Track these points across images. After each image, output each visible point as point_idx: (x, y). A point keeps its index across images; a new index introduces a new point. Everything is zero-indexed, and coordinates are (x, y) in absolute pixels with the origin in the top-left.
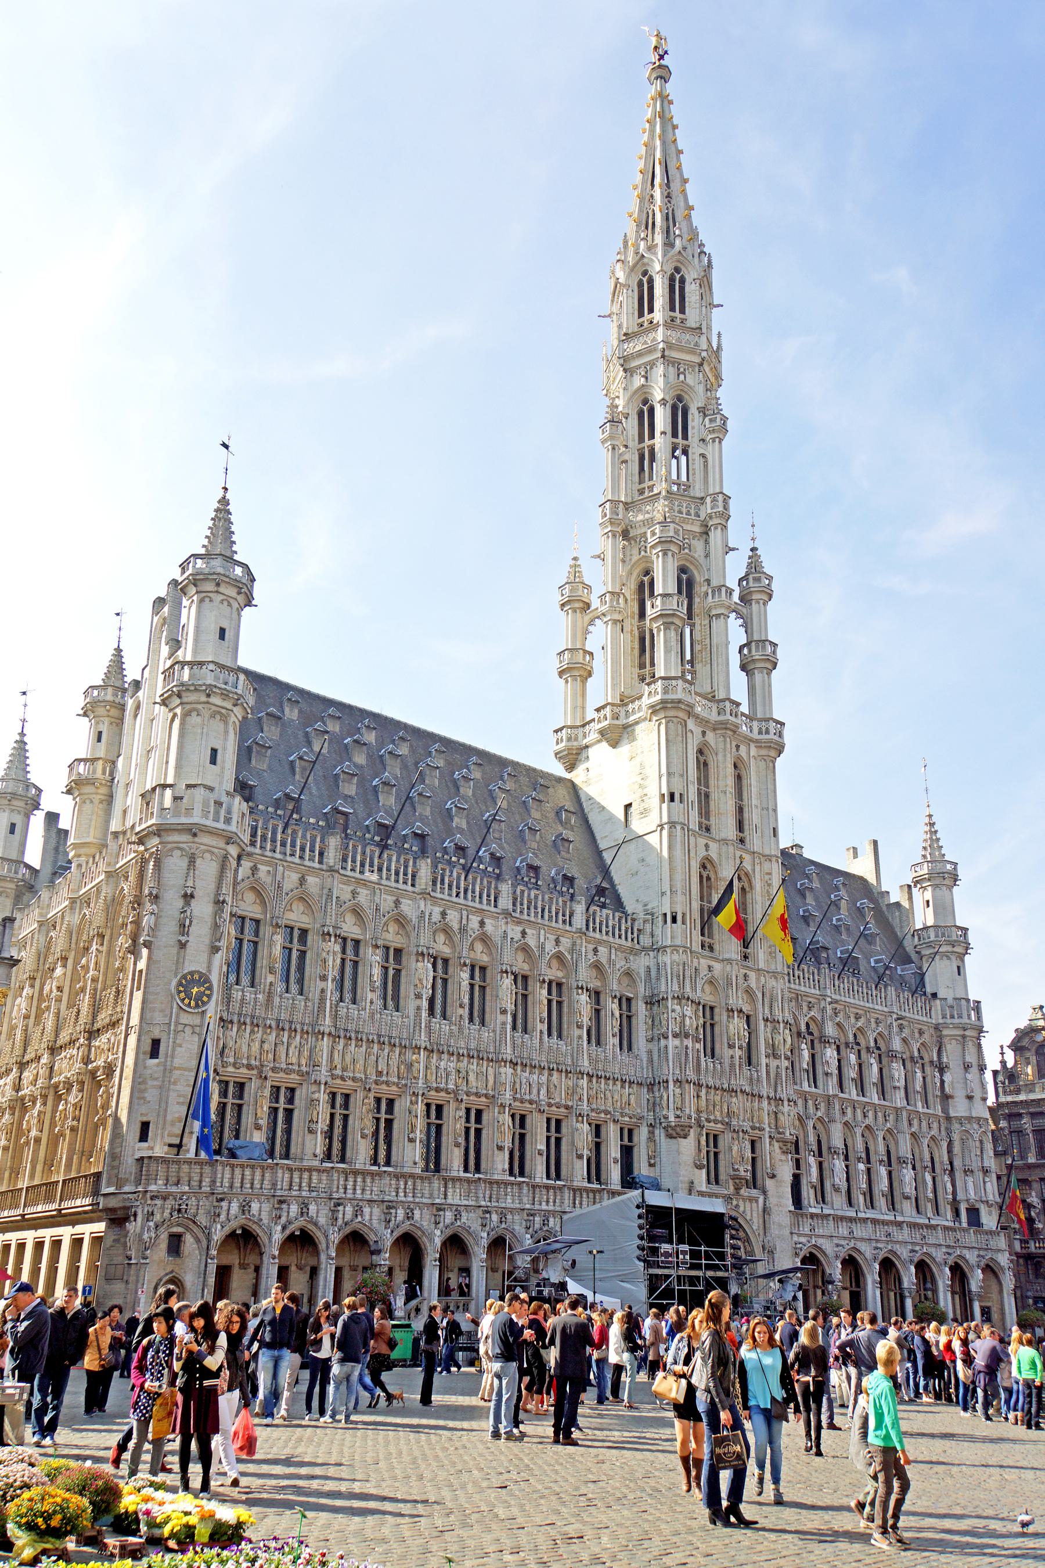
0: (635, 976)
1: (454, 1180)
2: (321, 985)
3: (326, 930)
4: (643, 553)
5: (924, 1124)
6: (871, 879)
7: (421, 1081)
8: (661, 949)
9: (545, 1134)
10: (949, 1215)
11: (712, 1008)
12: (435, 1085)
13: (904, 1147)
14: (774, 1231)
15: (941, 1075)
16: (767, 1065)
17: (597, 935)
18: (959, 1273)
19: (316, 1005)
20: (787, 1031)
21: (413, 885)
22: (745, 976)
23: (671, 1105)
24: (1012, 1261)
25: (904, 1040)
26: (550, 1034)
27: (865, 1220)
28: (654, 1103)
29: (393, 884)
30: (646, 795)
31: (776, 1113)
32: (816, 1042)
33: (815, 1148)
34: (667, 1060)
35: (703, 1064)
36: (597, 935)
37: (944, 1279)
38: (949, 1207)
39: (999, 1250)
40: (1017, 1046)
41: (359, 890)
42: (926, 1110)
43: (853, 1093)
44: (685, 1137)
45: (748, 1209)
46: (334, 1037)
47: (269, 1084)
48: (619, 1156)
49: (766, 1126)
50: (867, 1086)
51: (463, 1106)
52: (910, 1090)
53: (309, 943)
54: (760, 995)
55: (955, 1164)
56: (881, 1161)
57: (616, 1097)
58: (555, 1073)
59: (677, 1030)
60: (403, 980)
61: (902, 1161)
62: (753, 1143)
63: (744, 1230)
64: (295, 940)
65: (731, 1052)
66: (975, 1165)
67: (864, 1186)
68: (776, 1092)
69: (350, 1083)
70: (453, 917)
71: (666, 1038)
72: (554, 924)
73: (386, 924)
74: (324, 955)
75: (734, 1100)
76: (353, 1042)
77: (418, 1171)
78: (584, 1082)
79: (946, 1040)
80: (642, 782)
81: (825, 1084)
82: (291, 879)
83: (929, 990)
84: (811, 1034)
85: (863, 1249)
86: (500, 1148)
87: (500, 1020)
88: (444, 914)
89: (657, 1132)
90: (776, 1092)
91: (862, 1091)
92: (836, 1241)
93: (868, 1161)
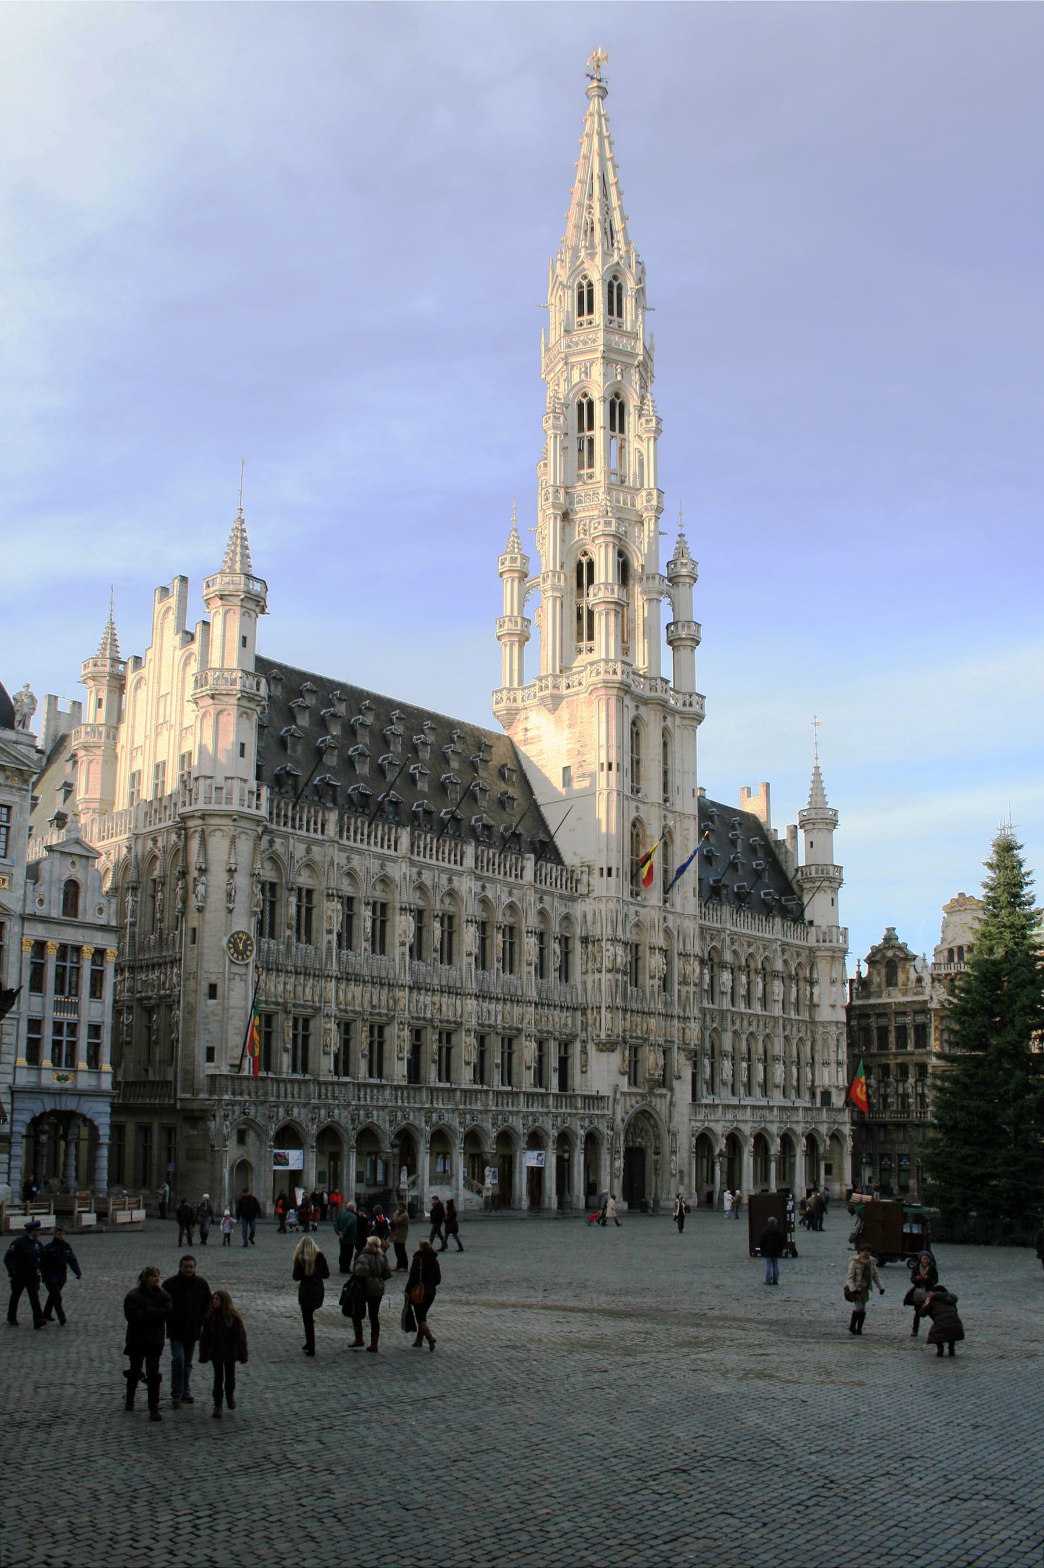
0: (573, 919)
1: (432, 1090)
2: (326, 937)
3: (330, 892)
5: (794, 1029)
6: (762, 819)
9: (500, 1050)
10: (807, 1097)
12: (416, 1015)
13: (778, 1047)
14: (676, 1118)
15: (811, 988)
16: (679, 991)
18: (812, 1140)
20: (697, 963)
21: (396, 850)
22: (665, 918)
24: (852, 1130)
25: (785, 962)
27: (745, 1107)
29: (379, 850)
32: (715, 967)
33: (709, 1052)
34: (600, 991)
36: (543, 887)
37: (801, 1147)
38: (808, 1092)
39: (844, 1123)
40: (871, 961)
41: (352, 856)
42: (797, 1017)
43: (742, 1007)
44: (613, 1051)
46: (338, 979)
47: (291, 1016)
48: (557, 1065)
49: (676, 1040)
51: (437, 1031)
52: (786, 1002)
54: (676, 933)
55: (816, 1058)
56: (759, 1060)
57: (557, 1019)
60: (388, 929)
61: (776, 1059)
62: (664, 1052)
63: (655, 1120)
64: (304, 900)
65: (652, 982)
66: (833, 1057)
67: (745, 1079)
68: (684, 1011)
70: (427, 877)
71: (600, 972)
72: (509, 879)
75: (653, 1020)
76: (353, 983)
77: (405, 1083)
78: (532, 1009)
79: (818, 960)
80: (581, 749)
81: (721, 1001)
82: (300, 850)
83: (808, 916)
84: (711, 960)
86: (468, 1063)
87: (465, 962)
88: (419, 874)
89: (589, 1046)
90: (684, 1011)
91: (749, 1004)
92: (723, 1123)
93: (749, 1059)
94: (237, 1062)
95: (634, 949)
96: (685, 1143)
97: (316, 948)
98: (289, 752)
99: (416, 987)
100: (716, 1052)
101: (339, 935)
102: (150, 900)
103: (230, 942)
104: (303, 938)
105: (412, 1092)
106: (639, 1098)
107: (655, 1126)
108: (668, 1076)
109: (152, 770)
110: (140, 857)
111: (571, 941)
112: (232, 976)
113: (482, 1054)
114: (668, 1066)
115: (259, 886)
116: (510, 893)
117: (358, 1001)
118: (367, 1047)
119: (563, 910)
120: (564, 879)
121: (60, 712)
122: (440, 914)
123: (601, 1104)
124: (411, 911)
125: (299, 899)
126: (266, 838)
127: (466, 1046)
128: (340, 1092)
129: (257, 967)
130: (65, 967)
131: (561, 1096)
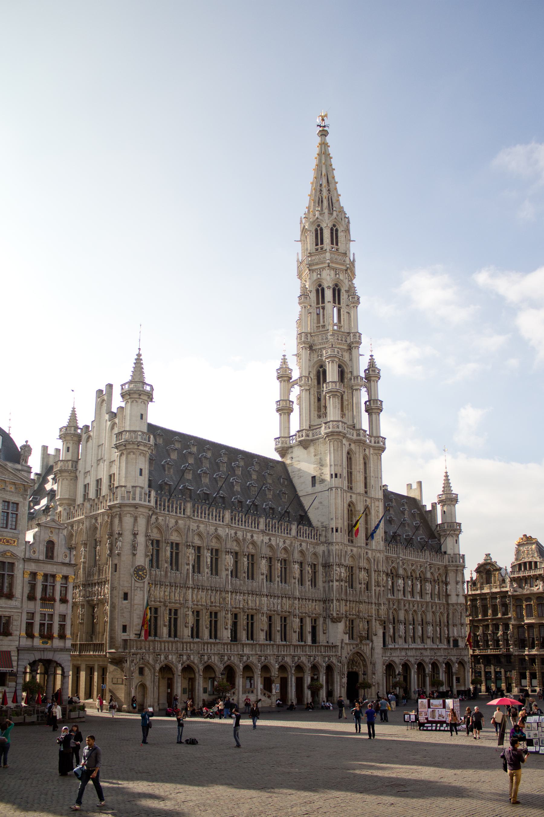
2: (187, 567)
4: (320, 358)
7: (229, 605)
8: (331, 543)
11: (352, 567)
14: (376, 656)
16: (375, 590)
17: (302, 538)
19: (185, 576)
20: (384, 575)
21: (223, 521)
23: (335, 610)
26: (281, 583)
27: (412, 649)
28: (326, 609)
29: (214, 522)
30: (323, 473)
31: (378, 610)
34: (333, 591)
35: (348, 591)
36: (302, 538)
41: (200, 525)
44: (340, 622)
45: (365, 648)
46: (193, 589)
47: (168, 608)
50: (415, 594)
53: (180, 549)
57: (310, 607)
58: (284, 599)
59: (338, 578)
60: (219, 563)
62: (368, 622)
64: (174, 548)
65: (360, 586)
68: (378, 600)
69: (200, 607)
70: (240, 534)
71: (332, 581)
73: (212, 539)
74: (188, 554)
75: (361, 606)
76: (201, 590)
78: (297, 602)
82: (172, 522)
85: (411, 660)
86: (262, 630)
87: (260, 578)
88: (236, 533)
89: (327, 620)
90: (378, 600)
94: (139, 633)
95: (351, 569)
96: (380, 669)
97: (181, 573)
98: (166, 472)
99: (235, 592)
100: (396, 621)
101: (193, 567)
102: (93, 550)
103: (135, 571)
104: (174, 568)
105: (232, 646)
106: (354, 646)
107: (364, 660)
108: (370, 634)
109: (95, 483)
110: (88, 528)
111: (317, 566)
112: (136, 588)
113: (270, 626)
114: (370, 629)
115: (150, 542)
116: (284, 542)
117: (204, 600)
118: (209, 623)
119: (311, 550)
120: (313, 534)
121: (49, 454)
122: (247, 554)
123: (334, 650)
124: (231, 553)
125: (172, 548)
126: (154, 517)
127: (262, 623)
128: (194, 647)
129: (149, 583)
130: (46, 585)
131: (313, 646)
